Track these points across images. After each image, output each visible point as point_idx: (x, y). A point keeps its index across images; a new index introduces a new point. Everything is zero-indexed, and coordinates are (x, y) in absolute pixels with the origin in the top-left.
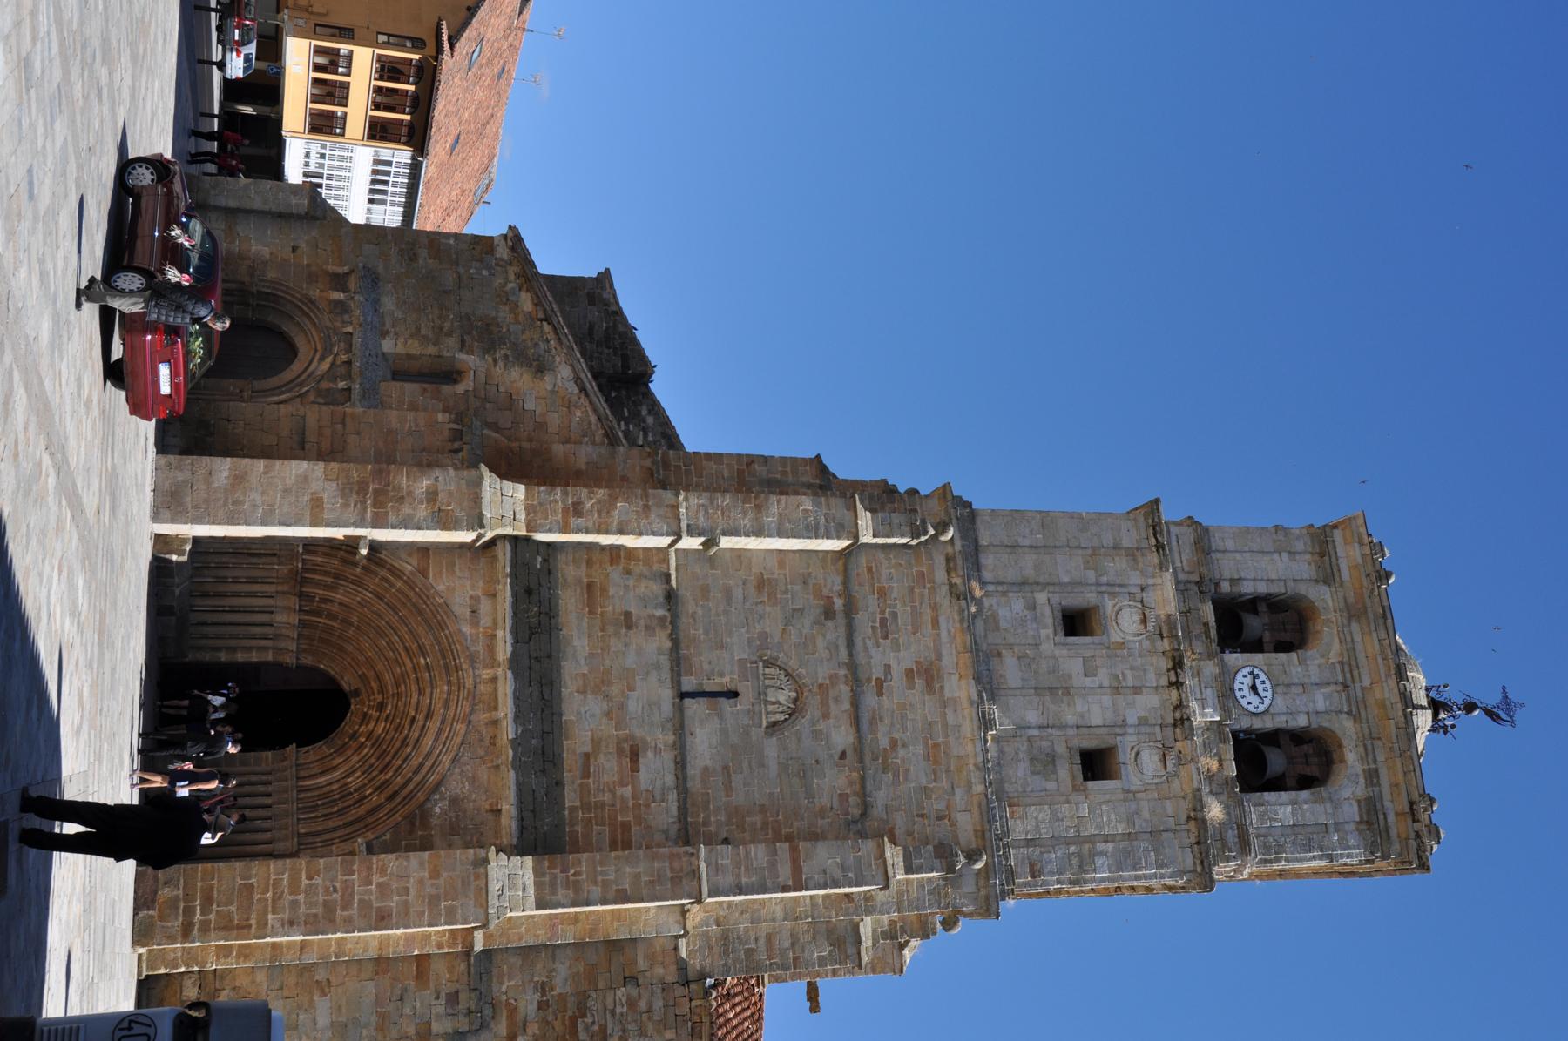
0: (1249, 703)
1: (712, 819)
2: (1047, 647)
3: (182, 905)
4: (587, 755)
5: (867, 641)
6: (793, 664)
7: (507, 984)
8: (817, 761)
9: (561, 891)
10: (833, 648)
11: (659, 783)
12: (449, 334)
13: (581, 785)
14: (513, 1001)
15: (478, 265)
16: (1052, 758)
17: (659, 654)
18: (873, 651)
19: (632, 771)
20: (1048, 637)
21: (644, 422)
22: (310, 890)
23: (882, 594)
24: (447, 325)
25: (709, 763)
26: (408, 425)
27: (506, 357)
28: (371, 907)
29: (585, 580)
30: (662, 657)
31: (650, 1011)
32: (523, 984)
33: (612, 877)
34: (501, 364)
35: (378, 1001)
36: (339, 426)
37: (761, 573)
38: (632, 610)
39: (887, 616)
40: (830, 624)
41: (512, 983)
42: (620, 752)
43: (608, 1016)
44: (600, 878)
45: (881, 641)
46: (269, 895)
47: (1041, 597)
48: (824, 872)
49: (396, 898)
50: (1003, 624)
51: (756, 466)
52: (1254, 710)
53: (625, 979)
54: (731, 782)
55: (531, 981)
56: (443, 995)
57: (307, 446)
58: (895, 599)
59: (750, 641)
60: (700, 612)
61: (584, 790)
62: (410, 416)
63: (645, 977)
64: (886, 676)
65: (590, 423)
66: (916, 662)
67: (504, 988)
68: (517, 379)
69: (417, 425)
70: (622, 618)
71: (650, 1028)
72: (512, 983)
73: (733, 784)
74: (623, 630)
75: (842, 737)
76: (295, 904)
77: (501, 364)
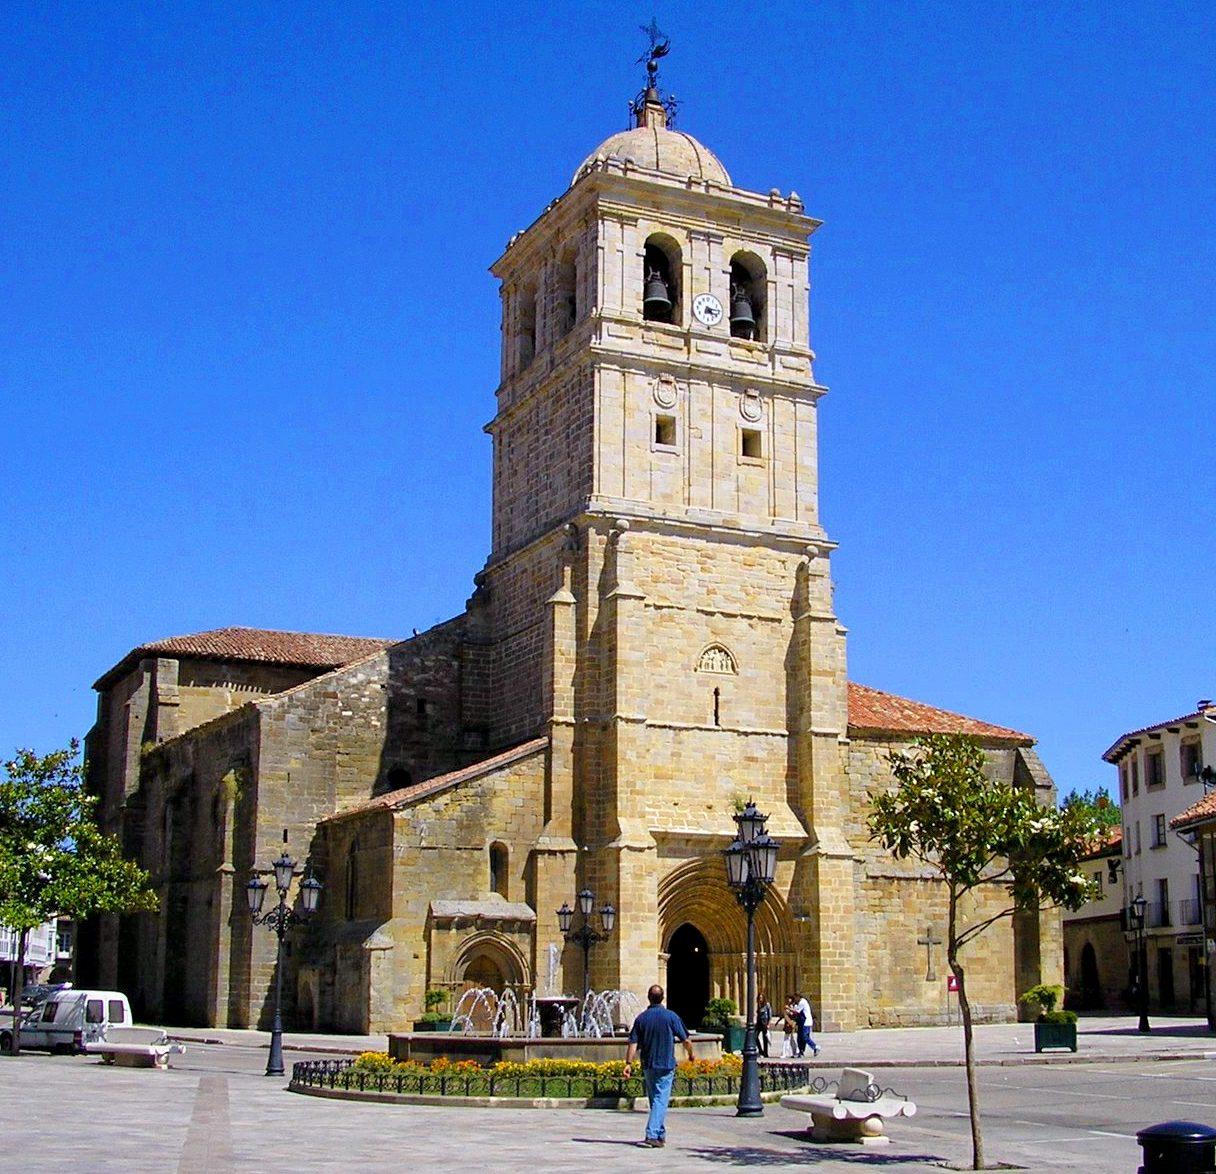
5: (686, 594)
21: (362, 682)
25: (753, 714)
29: (653, 780)
34: (491, 820)
42: (747, 768)
46: (836, 967)
49: (840, 903)
50: (668, 491)
68: (499, 805)
71: (869, 762)
77: (491, 820)
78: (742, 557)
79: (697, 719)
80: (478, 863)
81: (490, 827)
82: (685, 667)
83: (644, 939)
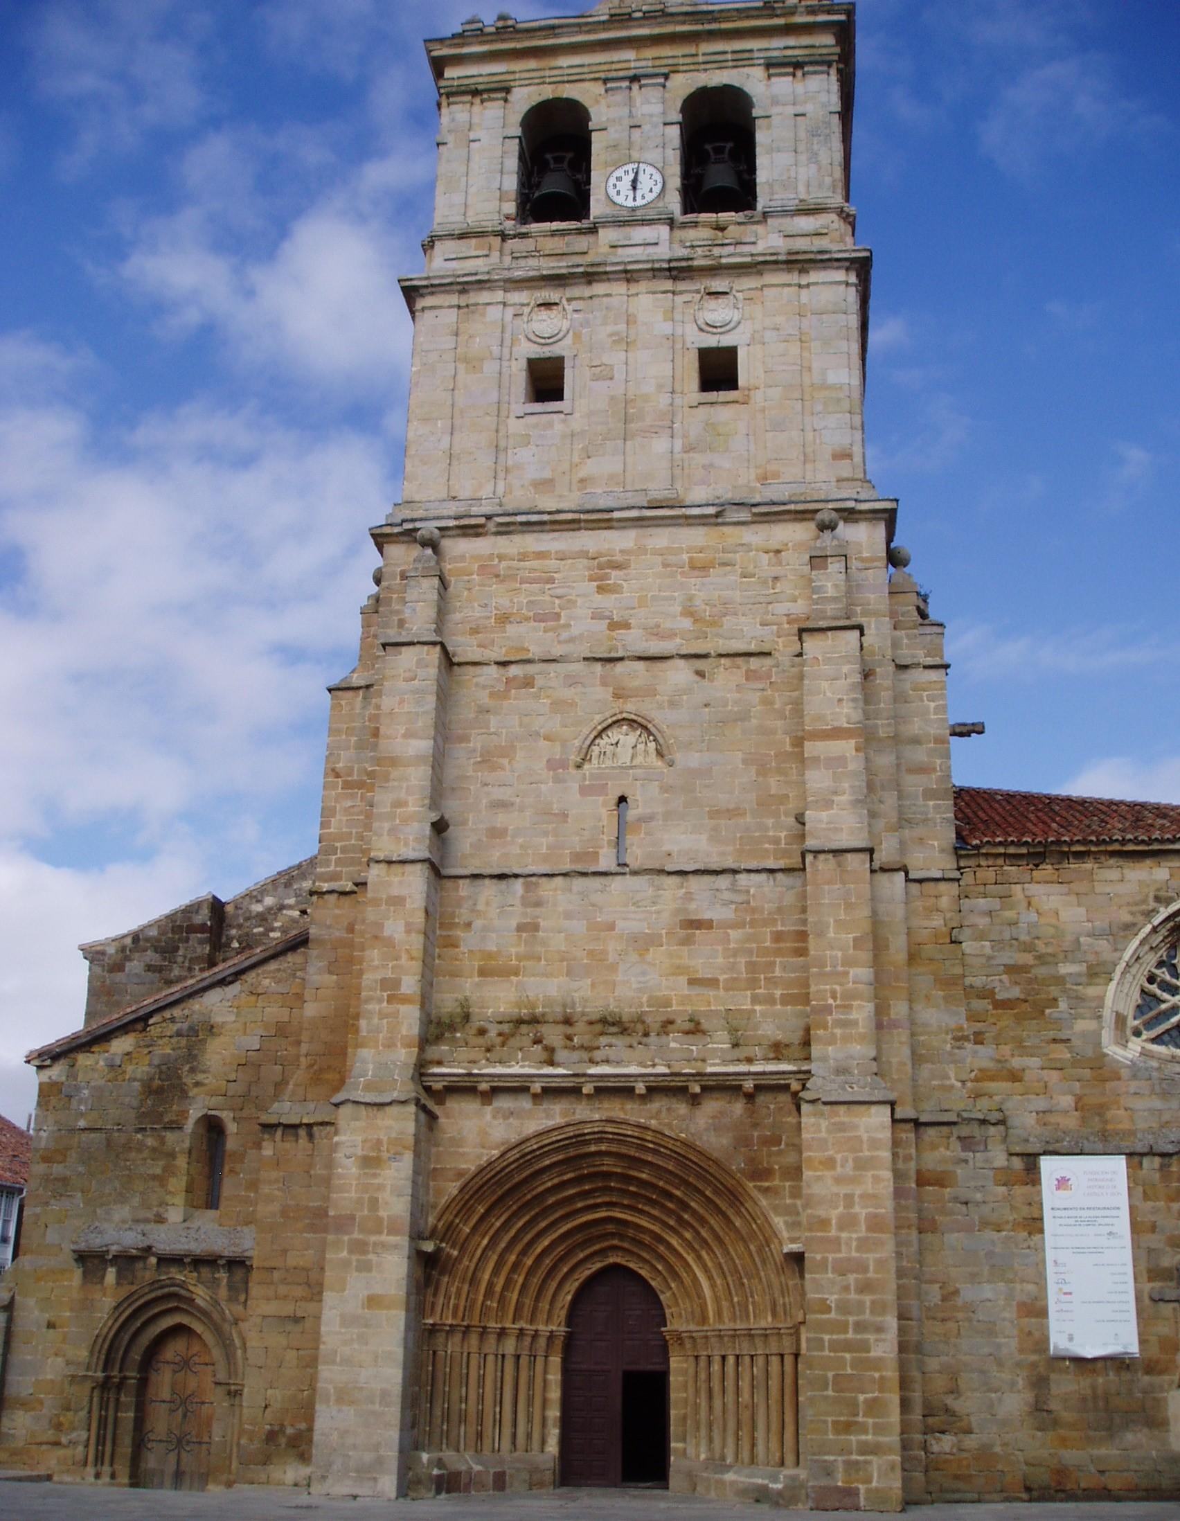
0: (651, 191)
1: (771, 834)
2: (577, 423)
3: (854, 1457)
4: (692, 982)
5: (562, 638)
6: (586, 731)
7: (953, 1081)
8: (707, 705)
9: (854, 1015)
10: (571, 680)
11: (727, 896)
12: (162, 1141)
13: (726, 989)
14: (973, 1074)
15: (74, 1102)
16: (710, 426)
17: (570, 890)
18: (575, 631)
19: (711, 927)
20: (564, 421)
22: (844, 1307)
23: (504, 619)
24: (150, 1142)
25: (704, 837)
26: (276, 1192)
27: (193, 1070)
28: (867, 1239)
29: (477, 979)
30: (575, 889)
31: (990, 913)
32: (955, 1062)
33: (840, 954)
34: (200, 1077)
35: (969, 1229)
36: (276, 1274)
37: (475, 763)
38: (513, 924)
39: (531, 614)
40: (539, 682)
41: (952, 1075)
42: (687, 941)
43: (994, 962)
44: (840, 969)
45: (562, 622)
46: (848, 1356)
47: (514, 426)
48: (840, 700)
49: (857, 1209)
50: (547, 474)
51: (341, 765)
52: (660, 186)
53: (952, 942)
54: (728, 810)
55: (951, 1054)
56: (963, 1155)
57: (299, 1314)
58: (511, 601)
59: (557, 780)
60: (520, 840)
61: (731, 985)
62: (265, 1189)
63: (951, 919)
64: (602, 618)
65: (279, 970)
66: (590, 580)
67: (959, 1084)
69: (277, 1181)
70: (524, 935)
71: (1010, 914)
72: (952, 1075)
73: (732, 806)
74: (540, 933)
75: (679, 674)
76: (860, 1327)
77: (200, 1077)
78: (685, 557)
79: (576, 857)
80: (172, 1155)
81: (195, 1091)
82: (552, 765)
83: (378, 1290)
